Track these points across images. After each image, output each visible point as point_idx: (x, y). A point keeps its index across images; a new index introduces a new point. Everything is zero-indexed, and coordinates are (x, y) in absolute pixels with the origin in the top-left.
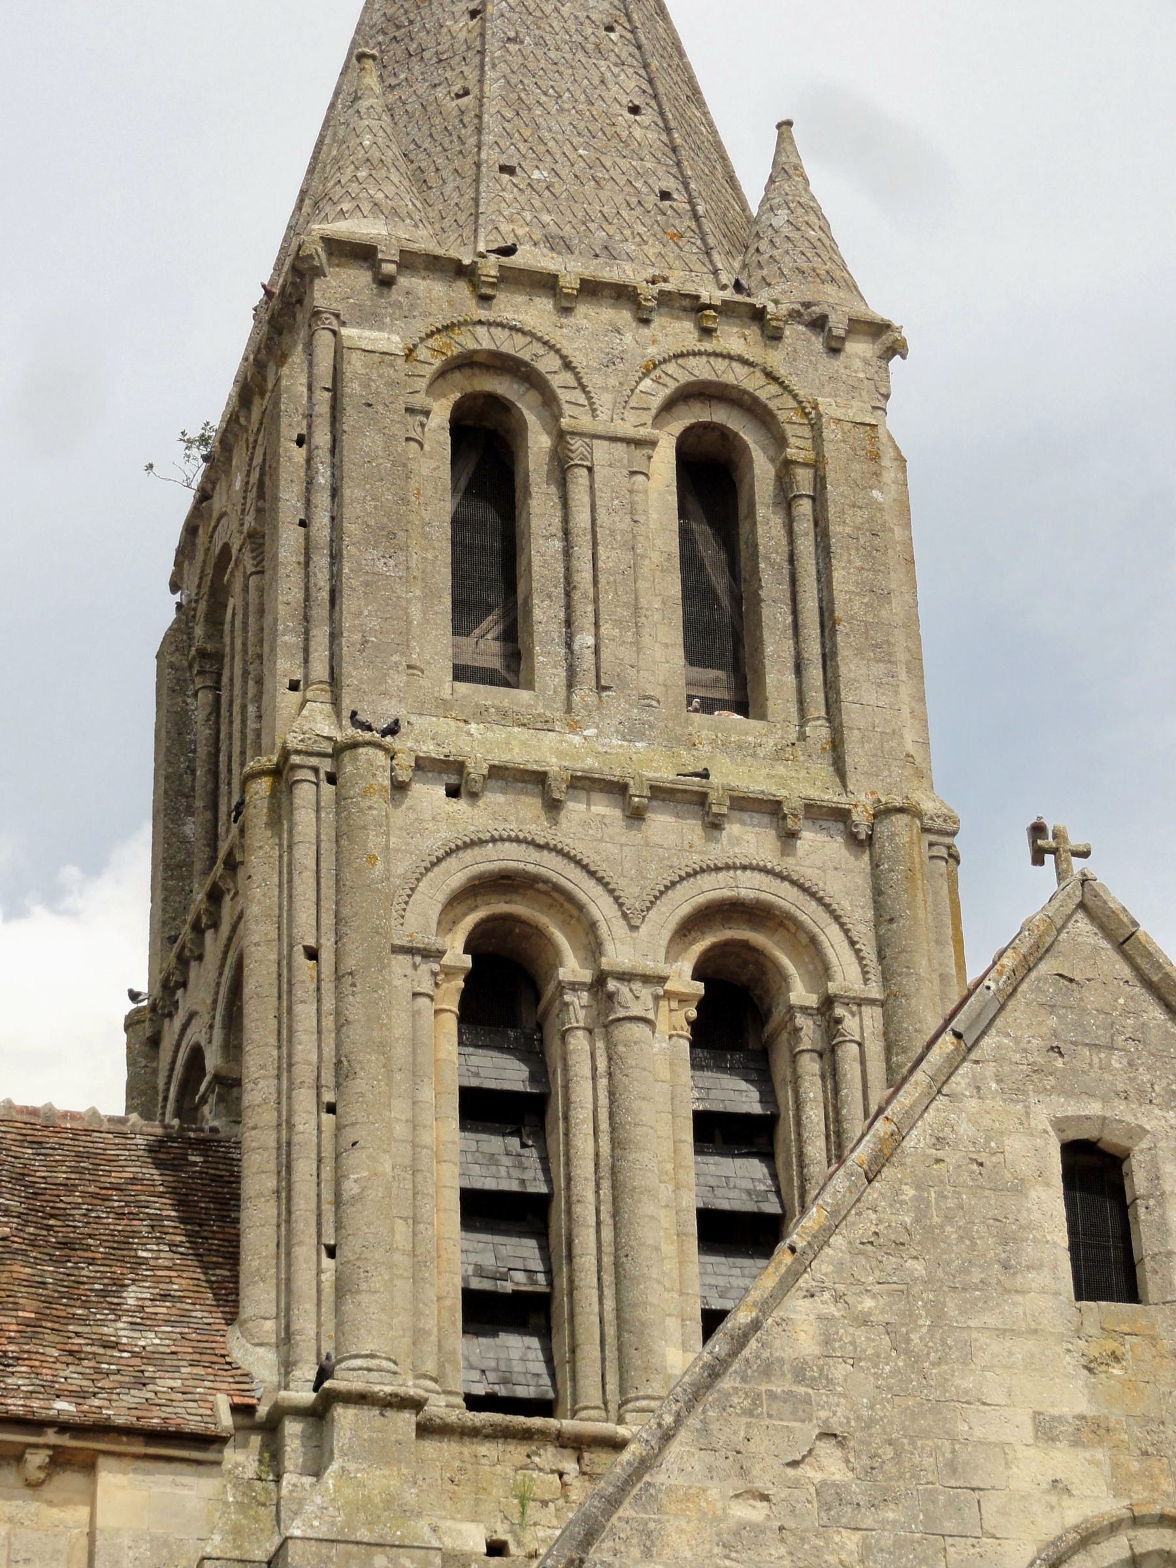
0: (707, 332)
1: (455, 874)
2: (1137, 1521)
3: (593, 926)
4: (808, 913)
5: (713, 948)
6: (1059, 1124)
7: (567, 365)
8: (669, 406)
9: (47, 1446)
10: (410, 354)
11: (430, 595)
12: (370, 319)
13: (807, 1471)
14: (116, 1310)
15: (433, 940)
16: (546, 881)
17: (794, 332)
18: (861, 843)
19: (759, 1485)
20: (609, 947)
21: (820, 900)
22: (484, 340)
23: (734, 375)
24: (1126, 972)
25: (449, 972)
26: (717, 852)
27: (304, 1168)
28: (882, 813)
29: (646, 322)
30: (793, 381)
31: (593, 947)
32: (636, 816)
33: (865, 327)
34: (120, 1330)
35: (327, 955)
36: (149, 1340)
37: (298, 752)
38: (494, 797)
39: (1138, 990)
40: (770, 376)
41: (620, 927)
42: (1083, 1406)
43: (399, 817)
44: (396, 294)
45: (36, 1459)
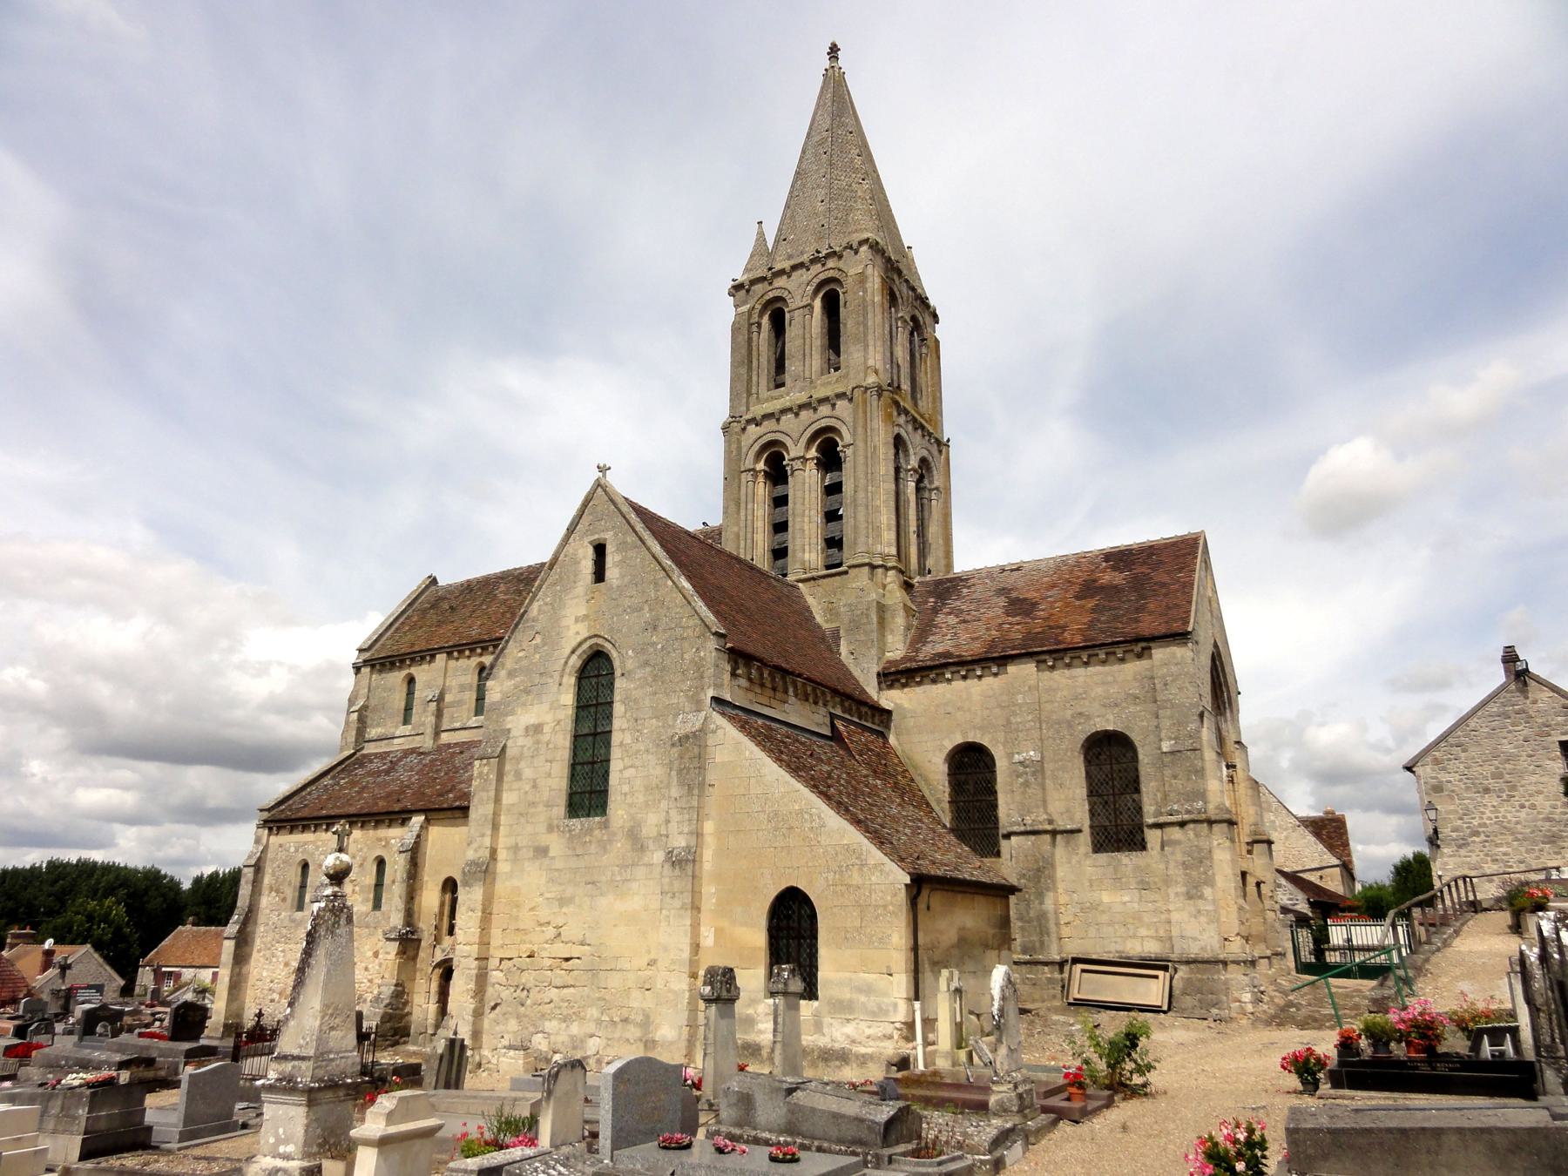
0: (823, 265)
1: (756, 447)
2: (590, 637)
5: (818, 445)
6: (591, 543)
12: (745, 303)
13: (534, 642)
15: (752, 467)
18: (851, 400)
22: (771, 295)
25: (760, 471)
26: (817, 416)
28: (853, 389)
29: (808, 270)
32: (797, 415)
38: (765, 423)
40: (840, 270)
42: (585, 613)
43: (744, 437)
44: (751, 293)
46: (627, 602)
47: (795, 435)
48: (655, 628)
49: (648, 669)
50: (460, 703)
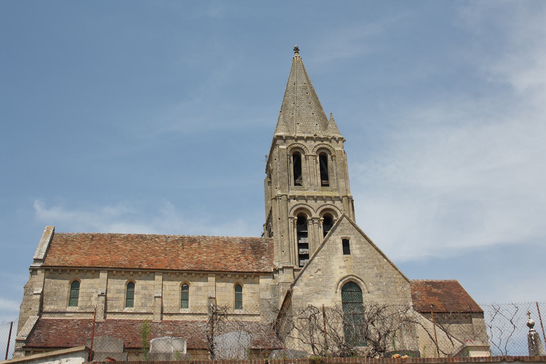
1: (295, 208)
3: (311, 213)
4: (335, 209)
6: (342, 238)
7: (306, 147)
8: (318, 150)
10: (287, 148)
12: (282, 144)
14: (261, 259)
16: (305, 208)
17: (333, 140)
19: (312, 274)
20: (312, 215)
21: (337, 207)
22: (296, 145)
23: (325, 146)
24: (348, 222)
27: (280, 243)
28: (343, 197)
30: (332, 146)
31: (311, 215)
34: (262, 261)
36: (265, 262)
37: (277, 196)
39: (350, 224)
41: (314, 213)
45: (253, 276)
46: (365, 265)
47: (315, 209)
48: (381, 276)
49: (380, 292)
50: (117, 299)
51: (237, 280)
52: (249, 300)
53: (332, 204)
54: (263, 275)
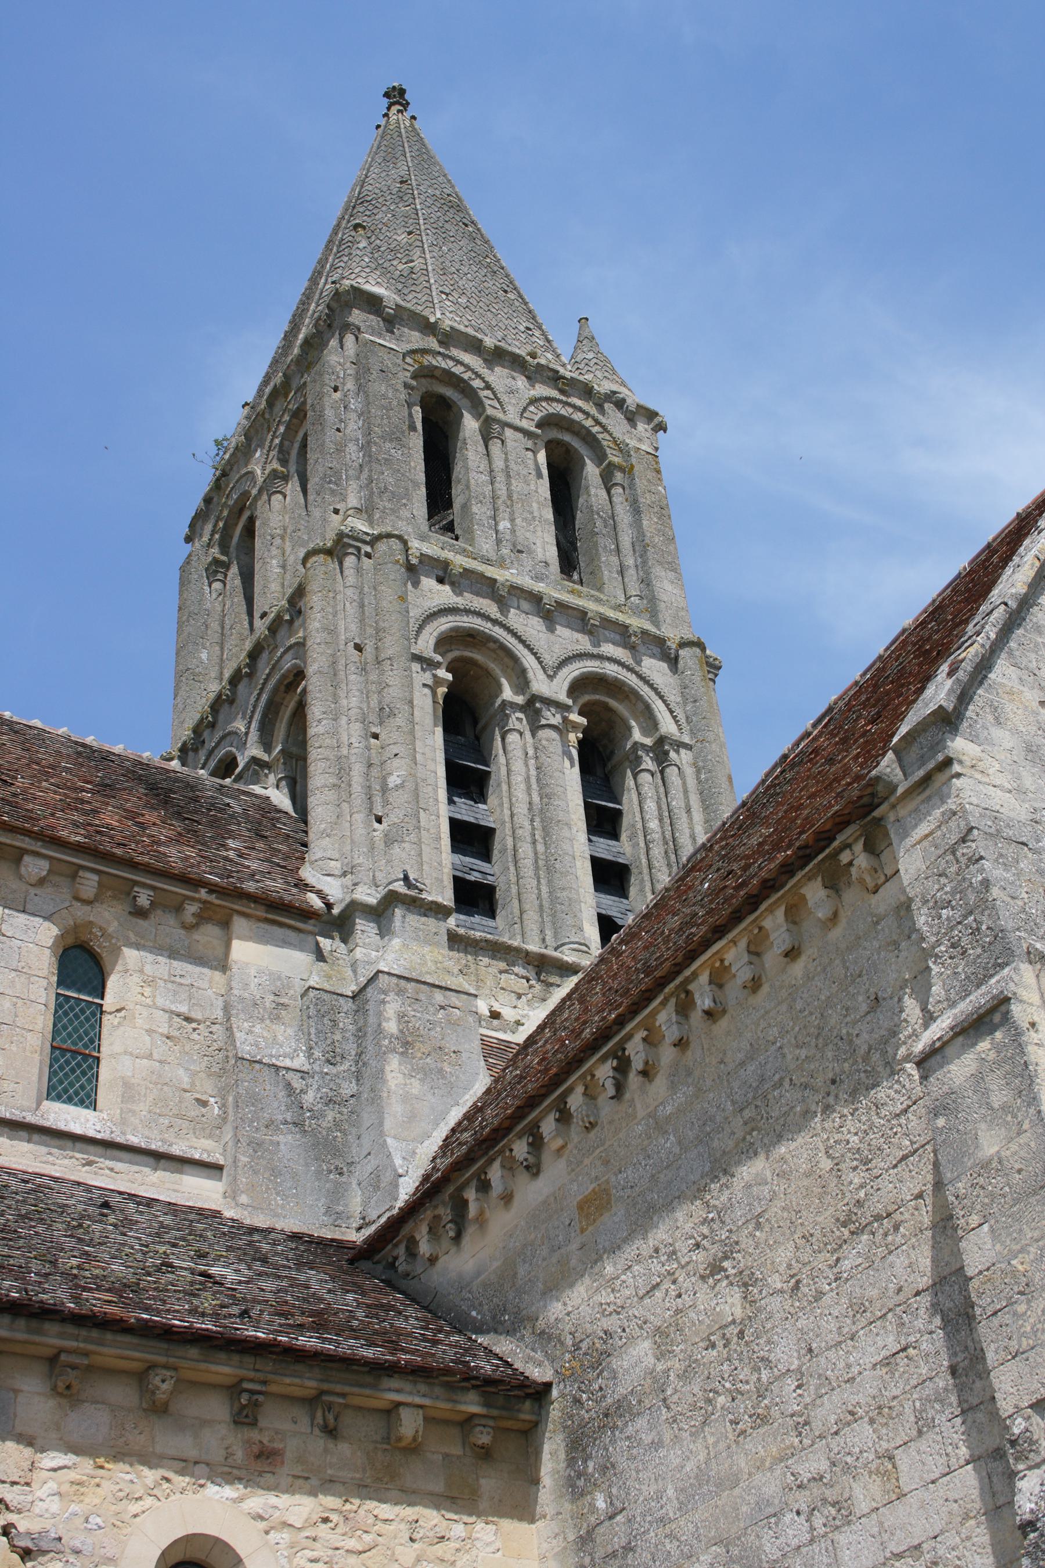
1: (445, 624)
3: (524, 671)
4: (645, 691)
9: (199, 900)
11: (416, 484)
28: (683, 644)
31: (522, 682)
33: (643, 411)
35: (369, 649)
37: (348, 536)
45: (191, 909)
51: (81, 912)
52: (149, 1057)
53: (630, 661)
54: (260, 919)
